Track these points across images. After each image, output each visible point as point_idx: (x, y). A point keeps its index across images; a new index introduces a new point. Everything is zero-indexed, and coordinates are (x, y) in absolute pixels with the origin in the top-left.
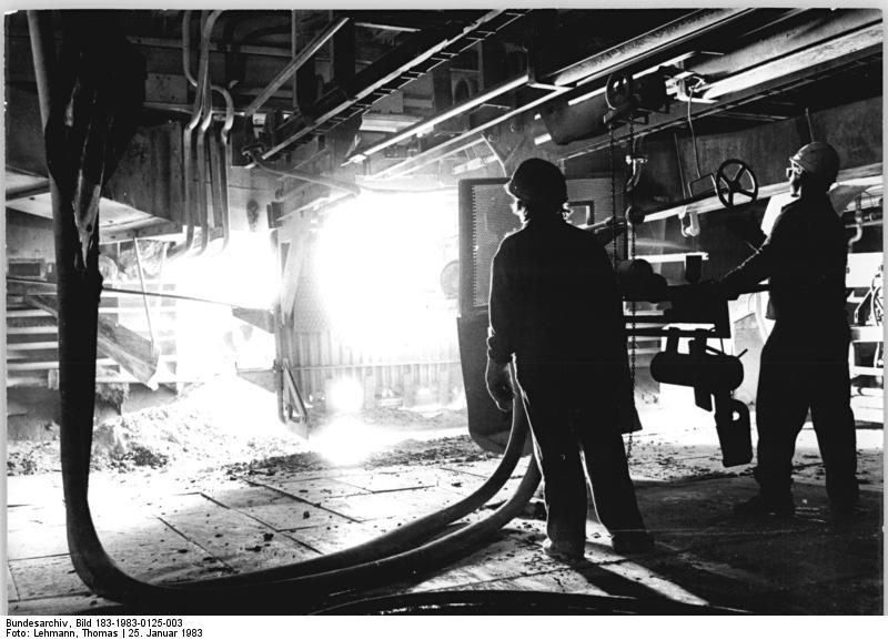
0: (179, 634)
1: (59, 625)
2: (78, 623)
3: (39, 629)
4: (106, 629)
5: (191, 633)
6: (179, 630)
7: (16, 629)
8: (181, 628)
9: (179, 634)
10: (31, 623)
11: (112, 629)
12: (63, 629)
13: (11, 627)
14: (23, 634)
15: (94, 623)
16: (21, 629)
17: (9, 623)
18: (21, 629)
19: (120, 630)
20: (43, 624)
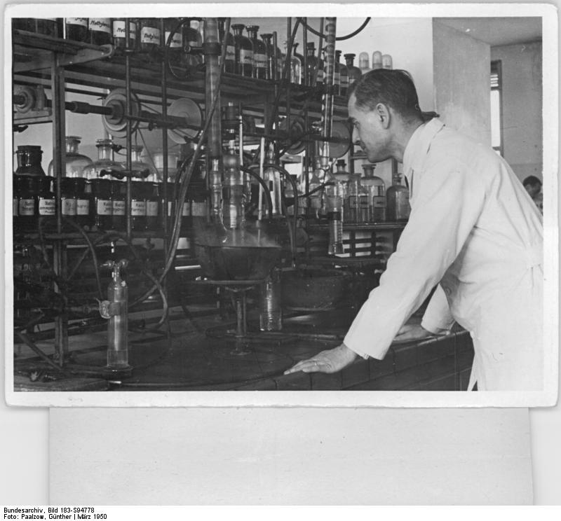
0: (92, 516)
1: (38, 511)
2: (49, 510)
3: (26, 514)
4: (66, 514)
5: (104, 516)
6: (90, 514)
7: (10, 514)
8: (94, 513)
9: (92, 516)
10: (20, 511)
11: (69, 514)
12: (40, 514)
13: (7, 513)
14: (15, 518)
15: (59, 510)
16: (13, 514)
17: (5, 510)
18: (13, 514)
19: (72, 514)
20: (27, 511)
